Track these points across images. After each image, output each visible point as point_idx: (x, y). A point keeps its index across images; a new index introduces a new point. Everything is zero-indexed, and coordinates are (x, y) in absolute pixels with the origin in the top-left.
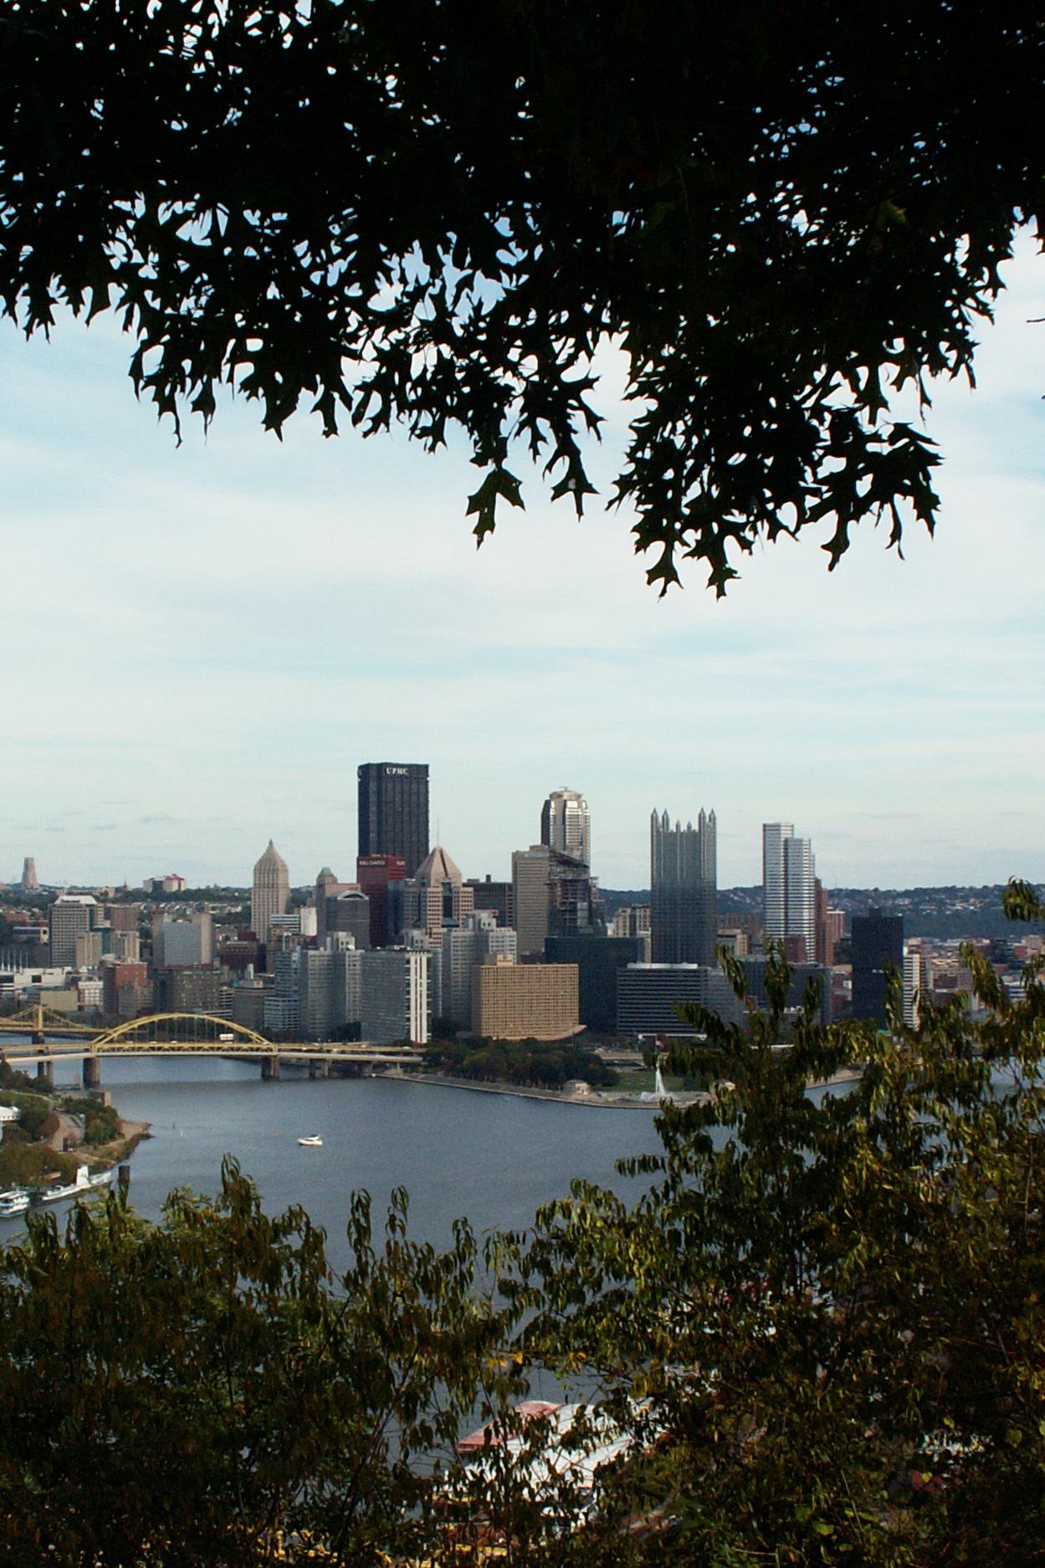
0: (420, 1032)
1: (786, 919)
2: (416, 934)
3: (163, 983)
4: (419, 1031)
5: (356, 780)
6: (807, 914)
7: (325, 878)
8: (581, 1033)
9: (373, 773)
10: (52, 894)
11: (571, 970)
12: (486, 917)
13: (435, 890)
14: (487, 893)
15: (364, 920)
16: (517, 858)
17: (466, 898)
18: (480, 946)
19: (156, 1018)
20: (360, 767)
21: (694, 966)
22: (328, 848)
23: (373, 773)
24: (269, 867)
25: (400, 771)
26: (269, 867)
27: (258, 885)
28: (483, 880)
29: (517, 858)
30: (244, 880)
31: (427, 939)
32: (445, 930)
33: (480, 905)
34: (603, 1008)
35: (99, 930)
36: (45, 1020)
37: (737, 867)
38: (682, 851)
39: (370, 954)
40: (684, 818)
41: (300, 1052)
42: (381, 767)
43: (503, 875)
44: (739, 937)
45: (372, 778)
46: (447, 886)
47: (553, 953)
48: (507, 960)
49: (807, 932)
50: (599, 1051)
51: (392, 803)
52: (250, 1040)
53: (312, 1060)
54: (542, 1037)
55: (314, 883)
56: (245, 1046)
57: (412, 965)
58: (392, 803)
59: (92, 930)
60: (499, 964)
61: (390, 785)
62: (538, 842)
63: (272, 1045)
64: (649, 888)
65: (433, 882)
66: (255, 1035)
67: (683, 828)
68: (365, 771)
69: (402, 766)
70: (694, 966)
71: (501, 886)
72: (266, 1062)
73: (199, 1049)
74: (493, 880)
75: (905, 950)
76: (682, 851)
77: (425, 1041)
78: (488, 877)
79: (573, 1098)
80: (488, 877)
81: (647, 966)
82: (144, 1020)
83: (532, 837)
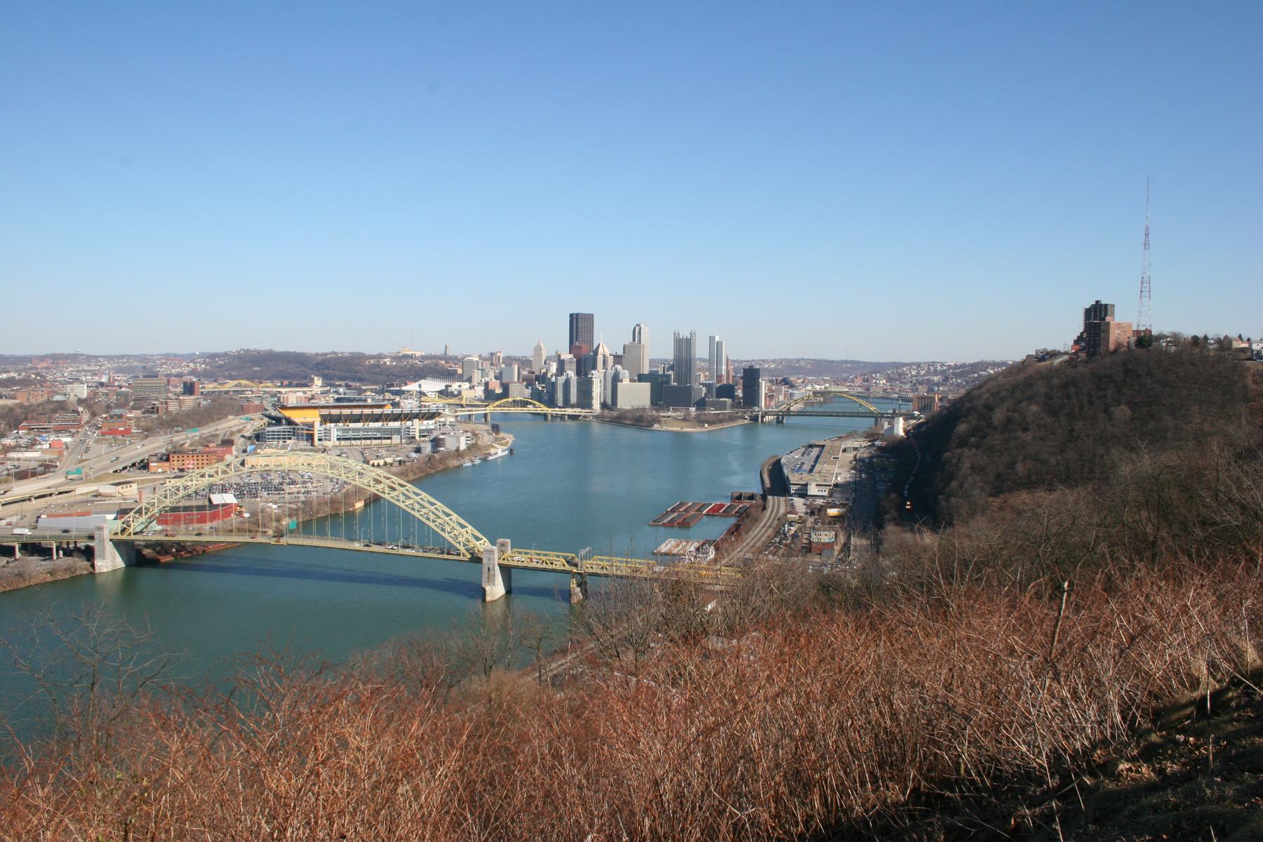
0: (596, 405)
6: (724, 367)
13: (600, 358)
14: (618, 359)
15: (574, 367)
17: (611, 359)
22: (558, 342)
24: (538, 349)
26: (538, 349)
37: (701, 351)
38: (684, 346)
40: (685, 334)
41: (557, 411)
43: (620, 353)
48: (626, 381)
49: (724, 373)
51: (579, 326)
58: (579, 326)
68: (571, 316)
72: (545, 415)
76: (684, 346)
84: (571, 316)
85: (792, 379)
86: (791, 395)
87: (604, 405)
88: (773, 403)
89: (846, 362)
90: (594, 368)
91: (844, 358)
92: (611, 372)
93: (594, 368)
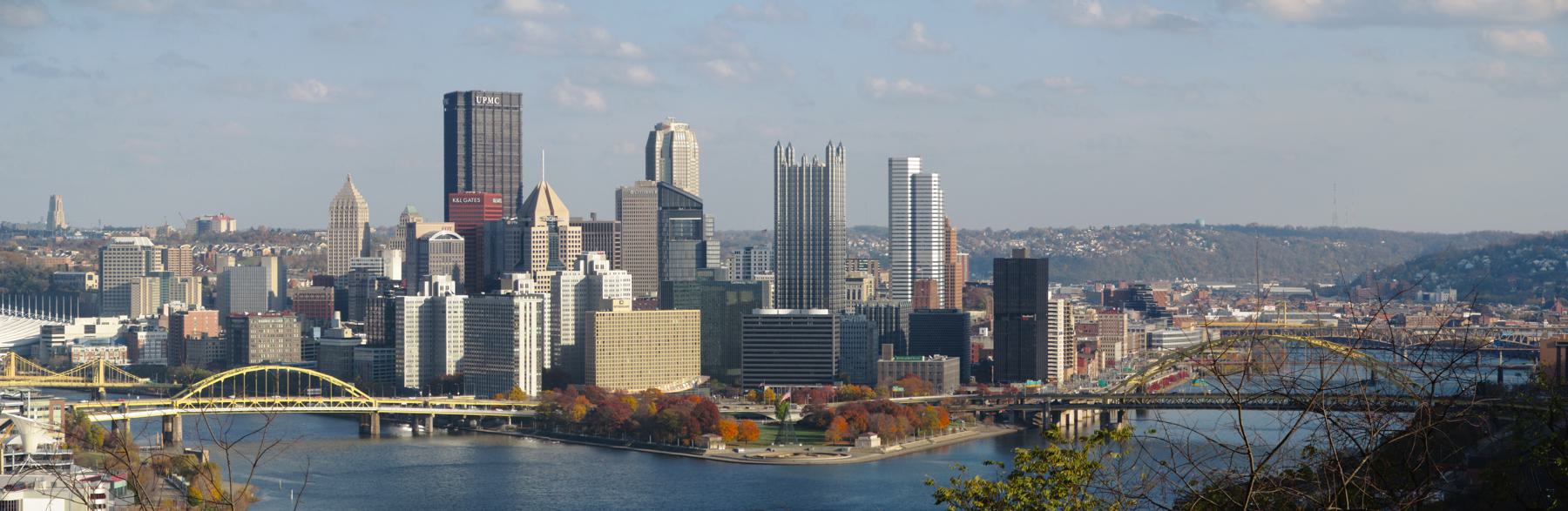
0: (529, 381)
1: (913, 262)
2: (521, 277)
3: (238, 332)
4: (528, 381)
5: (441, 110)
6: (937, 256)
8: (704, 385)
9: (461, 102)
12: (598, 259)
13: (539, 229)
14: (597, 234)
18: (590, 294)
19: (311, 372)
20: (446, 96)
21: (825, 312)
23: (461, 102)
24: (344, 209)
25: (491, 101)
28: (587, 219)
30: (319, 220)
31: (531, 283)
32: (553, 273)
33: (588, 245)
35: (156, 275)
36: (106, 375)
38: (805, 190)
39: (476, 300)
40: (806, 153)
41: (401, 406)
42: (468, 96)
43: (607, 214)
46: (554, 227)
47: (667, 299)
49: (937, 274)
52: (348, 395)
54: (666, 388)
55: (397, 222)
56: (342, 400)
57: (521, 312)
59: (149, 274)
60: (615, 310)
61: (480, 116)
63: (371, 400)
64: (771, 228)
65: (538, 221)
66: (352, 389)
68: (451, 99)
69: (493, 95)
70: (825, 312)
71: (607, 227)
72: (362, 419)
73: (335, 404)
74: (601, 218)
76: (805, 190)
77: (534, 394)
79: (708, 453)
80: (593, 215)
81: (774, 312)
84: (451, 99)
85: (1158, 289)
86: (1151, 341)
87: (549, 379)
88: (1092, 368)
89: (1336, 234)
90: (523, 265)
91: (1328, 223)
92: (571, 278)
93: (523, 265)
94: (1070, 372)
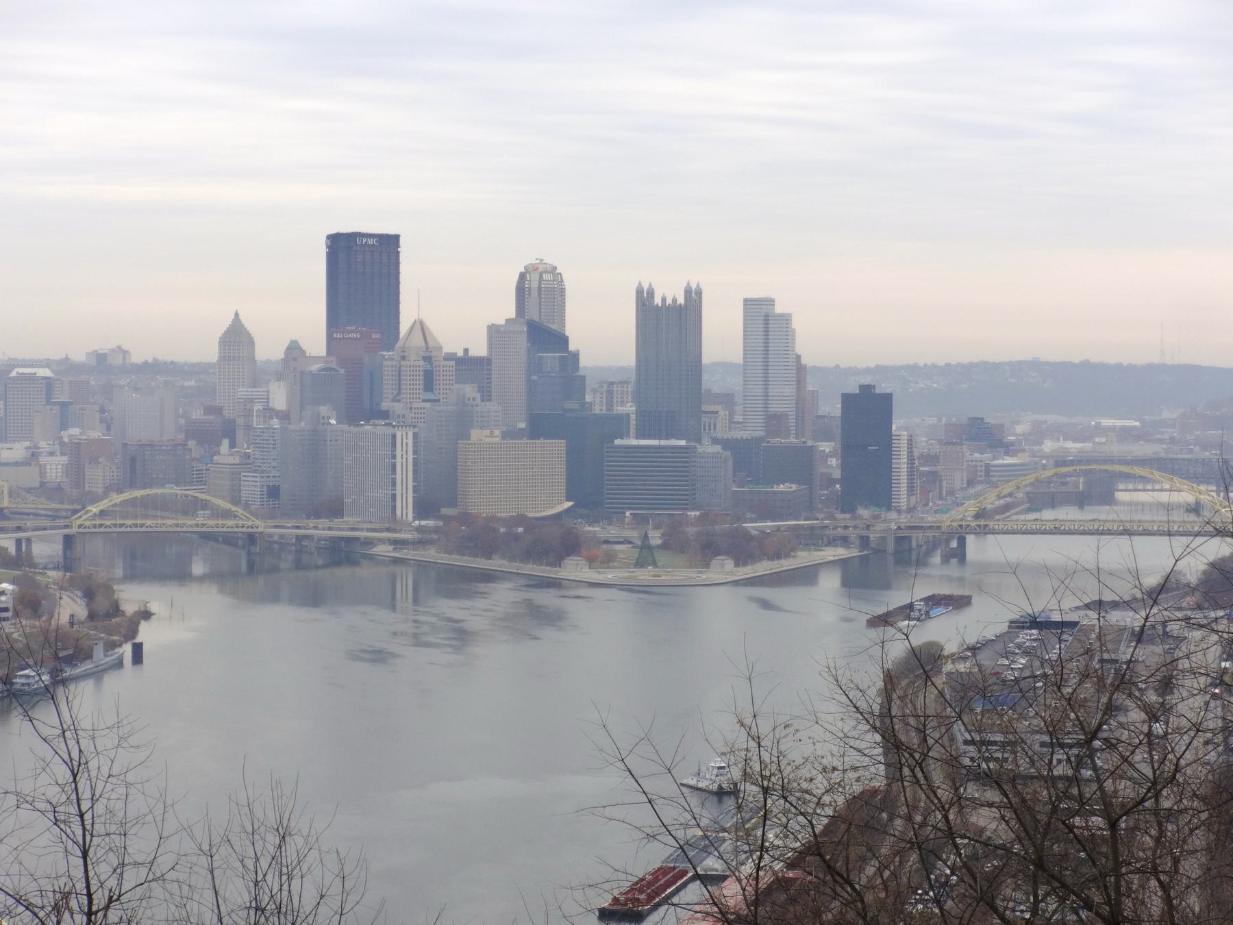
7: (294, 350)
8: (568, 511)
10: (868, 411)
11: (560, 445)
16: (493, 330)
20: (329, 237)
21: (683, 443)
25: (370, 241)
27: (224, 358)
28: (460, 354)
29: (493, 330)
34: (591, 486)
35: (55, 403)
36: (10, 496)
37: (722, 338)
38: (668, 326)
40: (670, 290)
43: (479, 348)
44: (721, 413)
45: (342, 248)
50: (794, 487)
53: (297, 537)
59: (48, 403)
62: (513, 315)
63: (258, 522)
65: (413, 358)
67: (669, 301)
70: (683, 443)
71: (478, 361)
74: (472, 353)
75: (894, 427)
78: (466, 351)
80: (466, 351)
82: (117, 498)
83: (506, 310)
94: (913, 499)
